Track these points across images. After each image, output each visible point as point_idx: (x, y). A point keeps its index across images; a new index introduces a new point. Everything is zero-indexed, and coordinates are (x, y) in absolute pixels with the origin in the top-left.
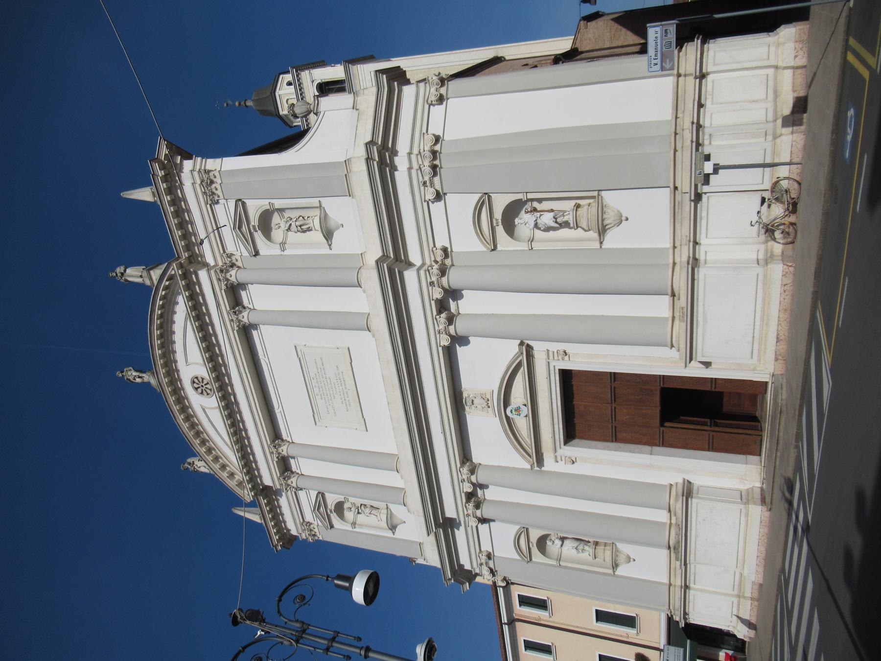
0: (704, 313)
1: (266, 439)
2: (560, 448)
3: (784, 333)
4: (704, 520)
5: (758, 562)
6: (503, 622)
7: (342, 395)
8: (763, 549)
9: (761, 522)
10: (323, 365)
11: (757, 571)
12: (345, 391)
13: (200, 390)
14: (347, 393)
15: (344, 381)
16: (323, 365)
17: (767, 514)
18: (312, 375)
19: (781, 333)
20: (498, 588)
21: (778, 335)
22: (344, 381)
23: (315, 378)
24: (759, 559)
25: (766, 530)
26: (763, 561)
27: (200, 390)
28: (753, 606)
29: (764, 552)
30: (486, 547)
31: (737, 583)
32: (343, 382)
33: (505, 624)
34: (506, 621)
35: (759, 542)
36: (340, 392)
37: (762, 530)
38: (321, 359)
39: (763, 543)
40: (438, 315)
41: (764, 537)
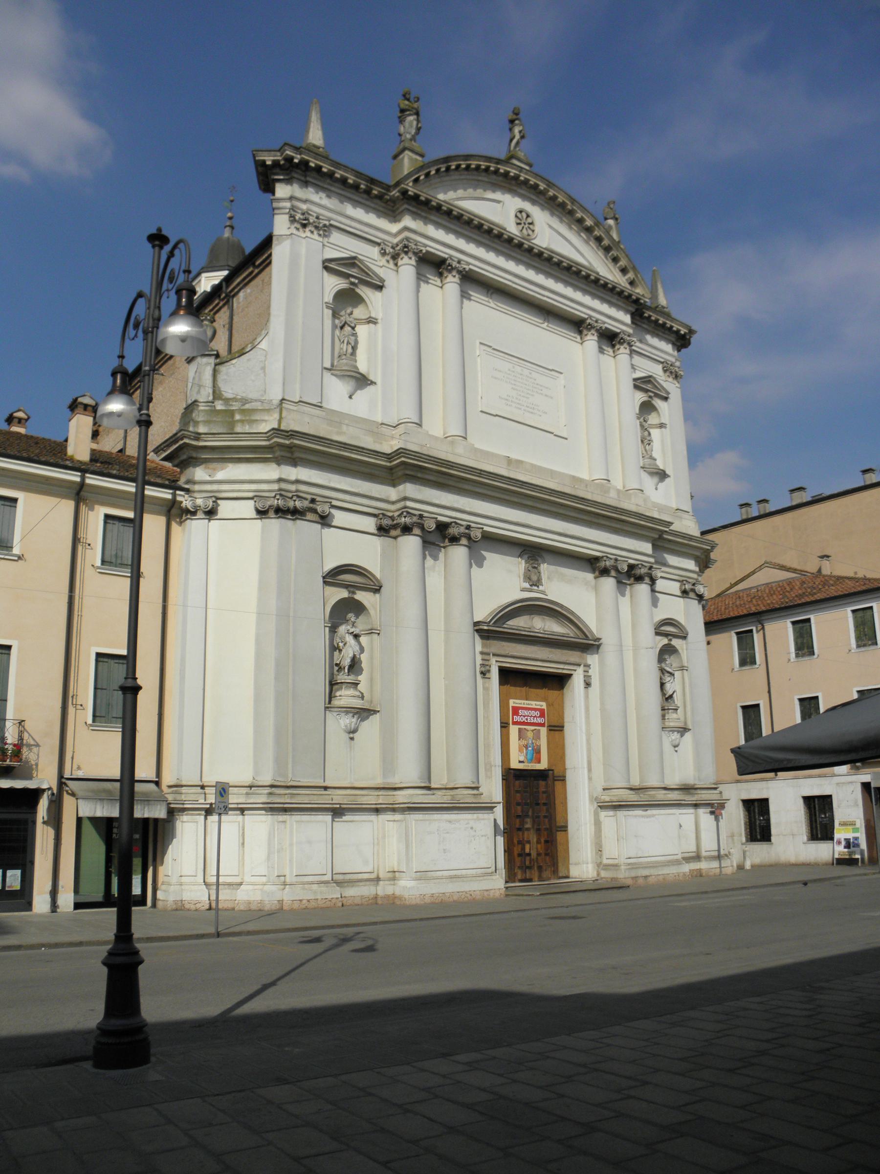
0: (653, 816)
1: (475, 266)
2: (496, 661)
3: (651, 880)
4: (472, 828)
5: (437, 895)
6: (87, 475)
7: (518, 401)
8: (455, 898)
9: (487, 890)
10: (546, 395)
11: (425, 895)
12: (523, 408)
13: (529, 220)
14: (520, 409)
15: (532, 413)
16: (546, 395)
17: (497, 894)
18: (534, 375)
19: (650, 879)
20: (171, 491)
21: (649, 876)
22: (532, 413)
23: (530, 376)
24: (441, 895)
25: (478, 897)
26: (440, 900)
27: (529, 220)
28: (334, 901)
29: (451, 900)
30: (339, 518)
31: (348, 877)
32: (530, 410)
33: (83, 478)
34: (88, 481)
35: (462, 892)
36: (520, 400)
37: (478, 892)
38: (552, 398)
39: (463, 897)
40: (629, 563)
41: (470, 897)
